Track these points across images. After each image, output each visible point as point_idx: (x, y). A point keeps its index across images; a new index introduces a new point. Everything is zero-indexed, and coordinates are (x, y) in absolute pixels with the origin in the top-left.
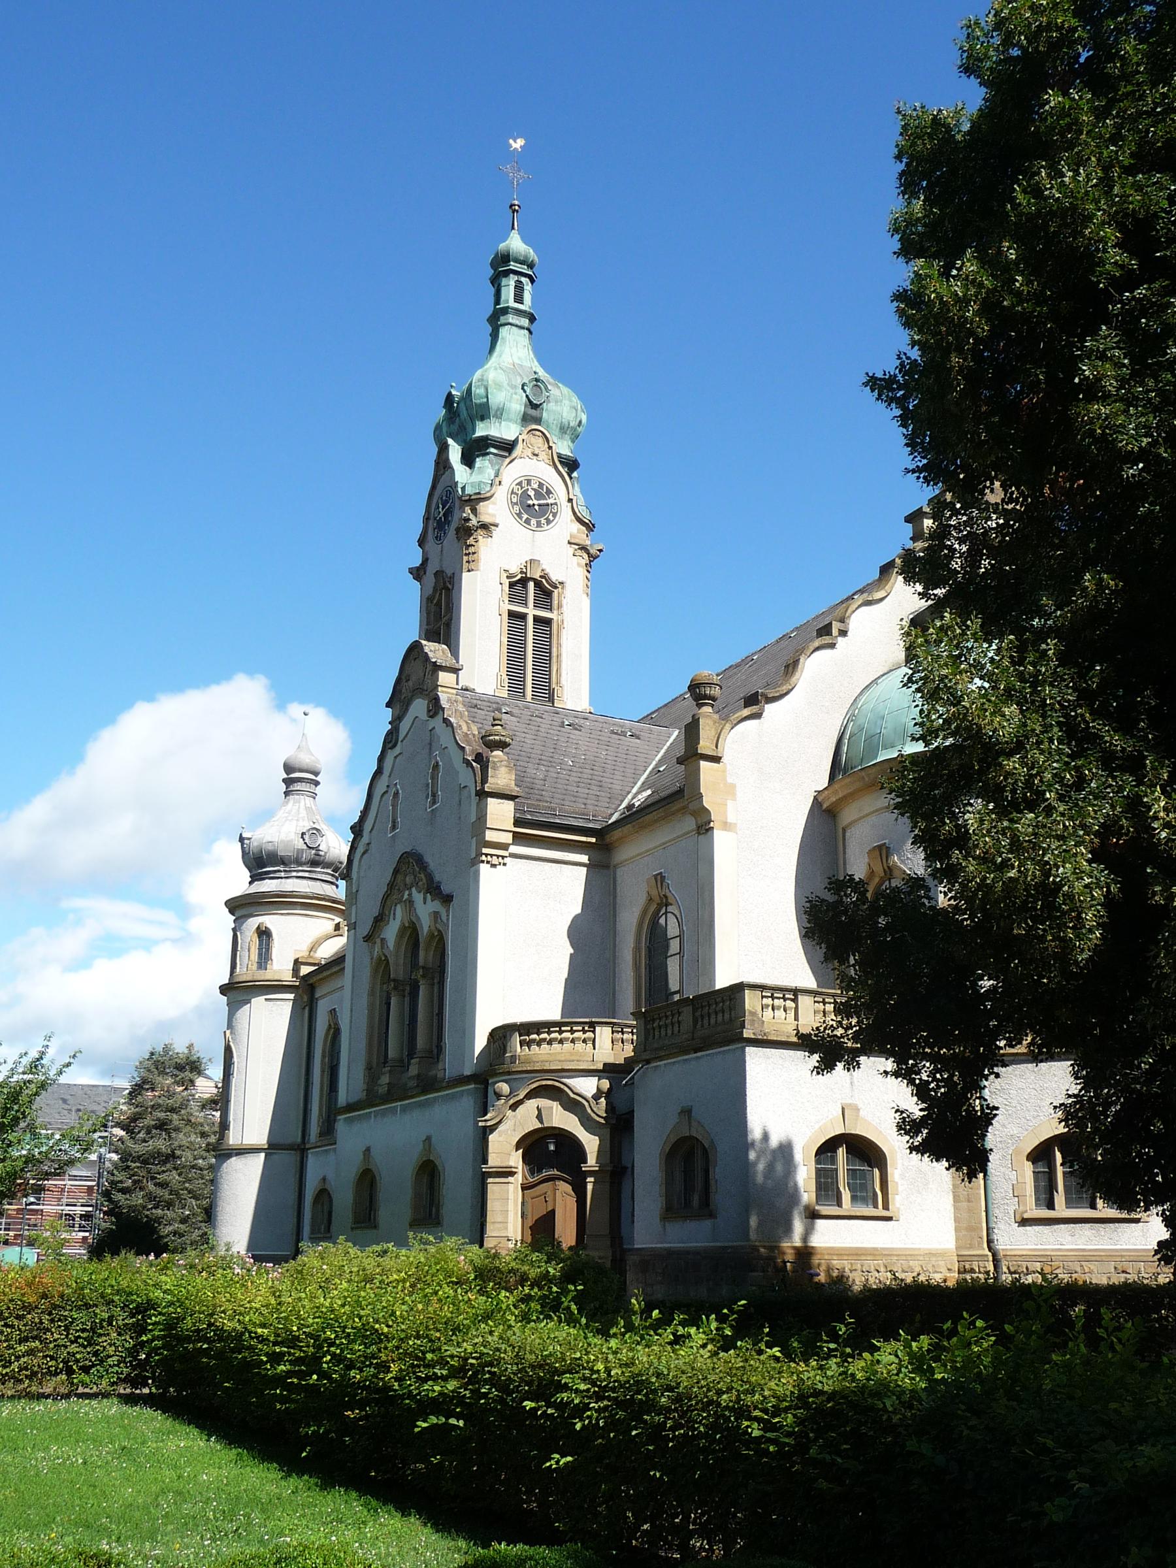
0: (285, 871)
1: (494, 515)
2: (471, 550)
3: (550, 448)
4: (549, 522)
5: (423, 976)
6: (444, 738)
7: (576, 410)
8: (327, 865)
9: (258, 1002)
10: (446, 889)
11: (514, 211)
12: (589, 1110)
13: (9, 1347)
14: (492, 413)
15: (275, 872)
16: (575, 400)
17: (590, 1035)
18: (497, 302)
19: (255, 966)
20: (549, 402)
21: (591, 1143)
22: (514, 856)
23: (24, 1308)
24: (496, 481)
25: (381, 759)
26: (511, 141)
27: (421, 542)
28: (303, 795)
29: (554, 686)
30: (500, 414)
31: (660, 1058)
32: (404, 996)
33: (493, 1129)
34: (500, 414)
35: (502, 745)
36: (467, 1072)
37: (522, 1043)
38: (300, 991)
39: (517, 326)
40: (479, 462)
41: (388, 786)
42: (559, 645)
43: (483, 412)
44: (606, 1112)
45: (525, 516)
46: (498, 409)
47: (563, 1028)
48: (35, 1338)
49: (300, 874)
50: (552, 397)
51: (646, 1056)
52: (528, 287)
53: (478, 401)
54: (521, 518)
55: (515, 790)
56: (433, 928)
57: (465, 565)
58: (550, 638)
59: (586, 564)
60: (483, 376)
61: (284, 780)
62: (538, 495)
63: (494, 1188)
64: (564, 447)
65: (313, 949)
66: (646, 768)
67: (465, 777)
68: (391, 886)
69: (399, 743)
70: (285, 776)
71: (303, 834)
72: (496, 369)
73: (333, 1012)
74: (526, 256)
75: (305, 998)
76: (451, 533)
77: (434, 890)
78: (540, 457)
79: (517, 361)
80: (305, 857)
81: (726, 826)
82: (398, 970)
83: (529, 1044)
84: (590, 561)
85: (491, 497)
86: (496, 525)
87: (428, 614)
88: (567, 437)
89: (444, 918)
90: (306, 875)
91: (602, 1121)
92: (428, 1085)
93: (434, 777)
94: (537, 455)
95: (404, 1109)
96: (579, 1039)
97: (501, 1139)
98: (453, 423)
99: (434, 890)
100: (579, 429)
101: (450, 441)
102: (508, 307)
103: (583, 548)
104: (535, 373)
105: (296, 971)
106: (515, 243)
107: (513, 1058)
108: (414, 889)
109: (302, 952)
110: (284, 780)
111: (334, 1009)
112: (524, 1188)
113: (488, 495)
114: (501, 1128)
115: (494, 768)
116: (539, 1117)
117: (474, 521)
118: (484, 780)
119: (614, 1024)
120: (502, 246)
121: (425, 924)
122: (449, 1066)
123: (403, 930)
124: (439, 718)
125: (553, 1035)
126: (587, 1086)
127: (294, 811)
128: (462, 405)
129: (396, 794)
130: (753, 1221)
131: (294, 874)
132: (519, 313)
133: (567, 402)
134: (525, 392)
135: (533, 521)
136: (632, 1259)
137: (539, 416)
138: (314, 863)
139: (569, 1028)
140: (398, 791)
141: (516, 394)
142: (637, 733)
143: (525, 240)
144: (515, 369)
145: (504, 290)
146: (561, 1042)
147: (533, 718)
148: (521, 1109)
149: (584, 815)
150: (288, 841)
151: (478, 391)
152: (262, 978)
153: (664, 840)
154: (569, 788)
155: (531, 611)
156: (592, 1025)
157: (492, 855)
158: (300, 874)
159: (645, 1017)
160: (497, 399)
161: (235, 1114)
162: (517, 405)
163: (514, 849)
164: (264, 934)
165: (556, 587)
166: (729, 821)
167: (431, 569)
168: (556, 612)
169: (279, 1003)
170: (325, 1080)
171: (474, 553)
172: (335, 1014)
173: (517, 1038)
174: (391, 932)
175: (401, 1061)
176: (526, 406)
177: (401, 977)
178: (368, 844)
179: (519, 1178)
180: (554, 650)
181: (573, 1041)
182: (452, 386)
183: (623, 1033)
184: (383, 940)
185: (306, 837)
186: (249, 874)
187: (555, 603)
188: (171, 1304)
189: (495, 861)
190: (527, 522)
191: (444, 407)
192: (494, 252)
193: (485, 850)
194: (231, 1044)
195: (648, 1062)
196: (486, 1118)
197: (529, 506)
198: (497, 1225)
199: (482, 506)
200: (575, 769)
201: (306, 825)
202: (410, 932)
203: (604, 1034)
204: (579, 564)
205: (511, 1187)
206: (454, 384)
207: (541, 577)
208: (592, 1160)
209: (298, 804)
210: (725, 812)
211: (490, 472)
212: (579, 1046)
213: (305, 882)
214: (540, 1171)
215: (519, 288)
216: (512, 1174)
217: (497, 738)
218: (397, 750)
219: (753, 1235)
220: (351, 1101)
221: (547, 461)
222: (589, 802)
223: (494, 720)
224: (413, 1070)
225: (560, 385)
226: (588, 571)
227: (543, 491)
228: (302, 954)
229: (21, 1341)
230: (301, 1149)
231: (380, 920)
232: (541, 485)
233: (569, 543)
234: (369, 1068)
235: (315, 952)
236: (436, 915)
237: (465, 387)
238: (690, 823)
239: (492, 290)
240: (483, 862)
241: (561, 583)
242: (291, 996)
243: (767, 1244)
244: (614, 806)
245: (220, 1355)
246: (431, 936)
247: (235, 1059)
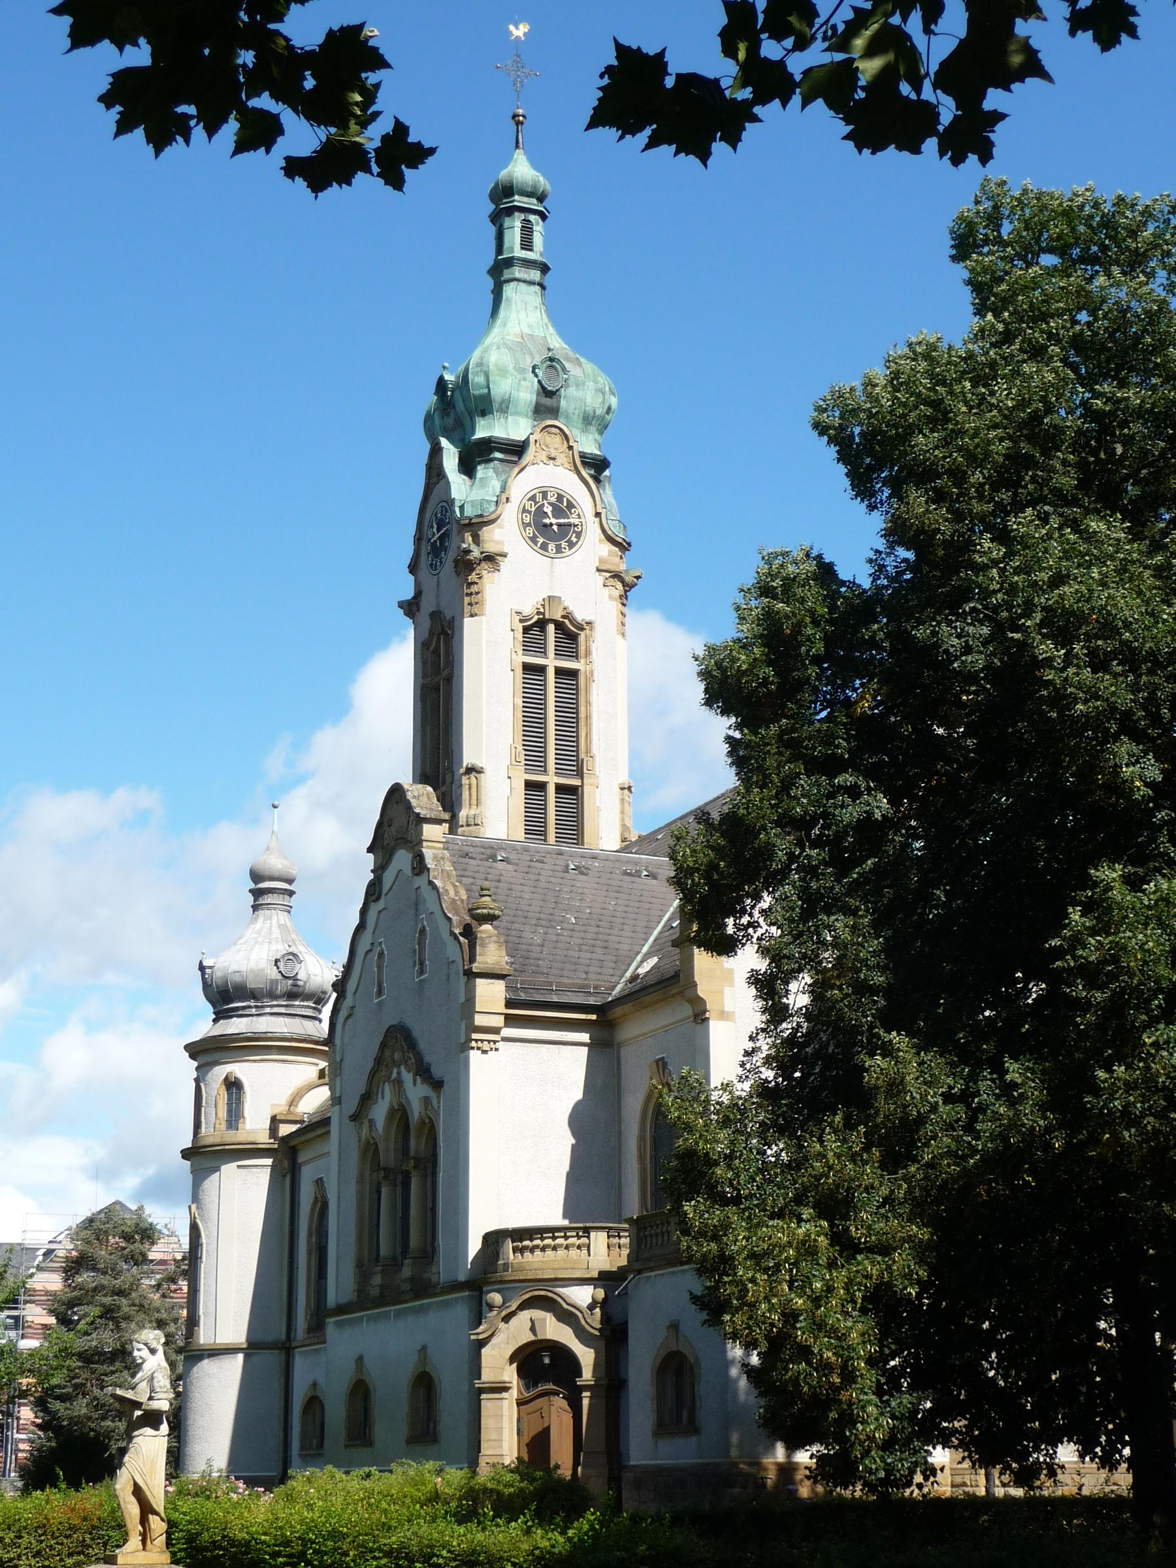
0: (256, 1007)
1: (501, 542)
2: (474, 589)
3: (570, 448)
4: (571, 545)
5: (416, 1167)
6: (430, 903)
7: (604, 394)
8: (308, 997)
9: (229, 1169)
10: (437, 1072)
11: (518, 123)
12: (583, 1322)
13: (61, 1560)
14: (495, 406)
15: (244, 1008)
16: (603, 380)
17: (584, 1240)
18: (500, 249)
19: (224, 1126)
20: (568, 386)
21: (586, 1356)
22: (505, 1039)
23: (70, 1529)
24: (502, 498)
25: (364, 912)
26: (512, 27)
27: (413, 568)
28: (275, 909)
29: (582, 755)
30: (505, 407)
31: (651, 1269)
32: (396, 1186)
33: (482, 1343)
34: (505, 407)
35: (490, 918)
36: (462, 1278)
37: (515, 1250)
38: (280, 1156)
39: (525, 281)
40: (481, 471)
41: (372, 944)
42: (588, 703)
43: (485, 406)
44: (602, 1323)
45: (541, 540)
46: (503, 401)
47: (556, 1234)
48: (79, 1553)
49: (275, 1010)
50: (572, 379)
51: (637, 1266)
52: (538, 227)
53: (477, 392)
54: (535, 543)
55: (506, 969)
56: (423, 1114)
57: (467, 609)
58: (577, 694)
59: (621, 596)
60: (482, 358)
61: (251, 891)
62: (558, 511)
63: (488, 1405)
64: (588, 444)
65: (293, 1102)
66: (661, 917)
67: (452, 951)
68: (378, 1061)
69: (383, 896)
70: (252, 886)
71: (277, 961)
72: (498, 348)
73: (319, 1182)
74: (535, 187)
75: (286, 1163)
76: (449, 565)
77: (424, 1072)
78: (558, 462)
79: (526, 330)
80: (281, 988)
81: (724, 1015)
82: (388, 1157)
83: (522, 1250)
84: (626, 591)
85: (498, 518)
86: (504, 555)
87: (424, 663)
88: (593, 429)
89: (435, 1105)
90: (283, 1010)
91: (597, 1333)
92: (423, 1288)
93: (421, 943)
94: (554, 459)
95: (398, 1314)
96: (573, 1245)
97: (494, 1353)
98: (448, 415)
99: (424, 1072)
100: (608, 417)
101: (444, 442)
102: (513, 258)
103: (617, 576)
104: (549, 349)
105: (273, 1130)
106: (521, 169)
107: (506, 1266)
108: (403, 1068)
109: (279, 1103)
110: (251, 891)
111: (321, 1179)
112: (520, 1403)
113: (493, 517)
114: (494, 1341)
115: (482, 946)
116: (533, 1329)
117: (476, 553)
118: (472, 959)
119: (610, 1228)
120: (503, 174)
121: (416, 1111)
122: (443, 1271)
123: (392, 1113)
124: (424, 877)
125: (547, 1242)
126: (582, 1296)
127: (265, 930)
128: (457, 395)
129: (381, 955)
130: (735, 1438)
131: (268, 1010)
132: (528, 264)
133: (591, 384)
134: (536, 376)
135: (552, 546)
136: (627, 1476)
137: (555, 405)
138: (292, 995)
139: (563, 1234)
140: (383, 950)
141: (525, 379)
142: (655, 871)
143: (535, 164)
144: (522, 345)
145: (507, 235)
146: (555, 1248)
147: (534, 864)
148: (514, 1321)
149: (582, 989)
150: (259, 970)
151: (477, 379)
152: (234, 1140)
153: (665, 1023)
154: (571, 953)
155: (551, 662)
156: (587, 1231)
157: (482, 1041)
158: (275, 1010)
159: (637, 1224)
160: (501, 388)
161: (206, 1306)
162: (527, 394)
163: (507, 1032)
164: (233, 1086)
165: (582, 629)
166: (726, 1009)
167: (427, 605)
168: (583, 661)
169: (254, 1170)
170: (313, 1263)
171: (477, 593)
172: (323, 1185)
173: (509, 1245)
174: (380, 1112)
175: (394, 1258)
176: (538, 394)
177: (391, 1163)
178: (352, 1008)
179: (514, 1393)
180: (582, 709)
181: (567, 1247)
182: (444, 367)
183: (620, 1237)
184: (371, 1122)
185: (281, 964)
186: (212, 1010)
187: (582, 648)
188: (190, 1522)
189: (486, 1046)
190: (544, 547)
191: (436, 393)
192: (495, 181)
193: (474, 1036)
194: (198, 1221)
195: (640, 1272)
196: (478, 1330)
197: (545, 525)
198: (490, 1443)
199: (485, 533)
200: (577, 928)
201: (280, 949)
202: (400, 1114)
203: (599, 1240)
204: (611, 597)
205: (505, 1403)
206: (447, 365)
207: (563, 617)
208: (587, 1374)
209: (273, 920)
210: (722, 1000)
211: (495, 484)
212: (574, 1252)
213: (281, 1019)
214: (535, 1385)
215: (527, 230)
216: (506, 1389)
217: (485, 911)
218: (381, 905)
219: (734, 1452)
220: (341, 1301)
221: (567, 466)
222: (592, 969)
223: (482, 889)
224: (407, 1272)
225: (582, 360)
226: (624, 605)
227: (563, 506)
228: (281, 1108)
229: (70, 1555)
230: (287, 1348)
231: (367, 1099)
232: (560, 498)
233: (598, 570)
234: (360, 1265)
235: (296, 1106)
236: (426, 1100)
237: (462, 368)
238: (687, 1010)
239: (492, 230)
240: (473, 1048)
241: (588, 623)
242: (269, 1161)
243: (746, 1460)
244: (619, 973)
245: (234, 1558)
246: (422, 1123)
247: (204, 1240)
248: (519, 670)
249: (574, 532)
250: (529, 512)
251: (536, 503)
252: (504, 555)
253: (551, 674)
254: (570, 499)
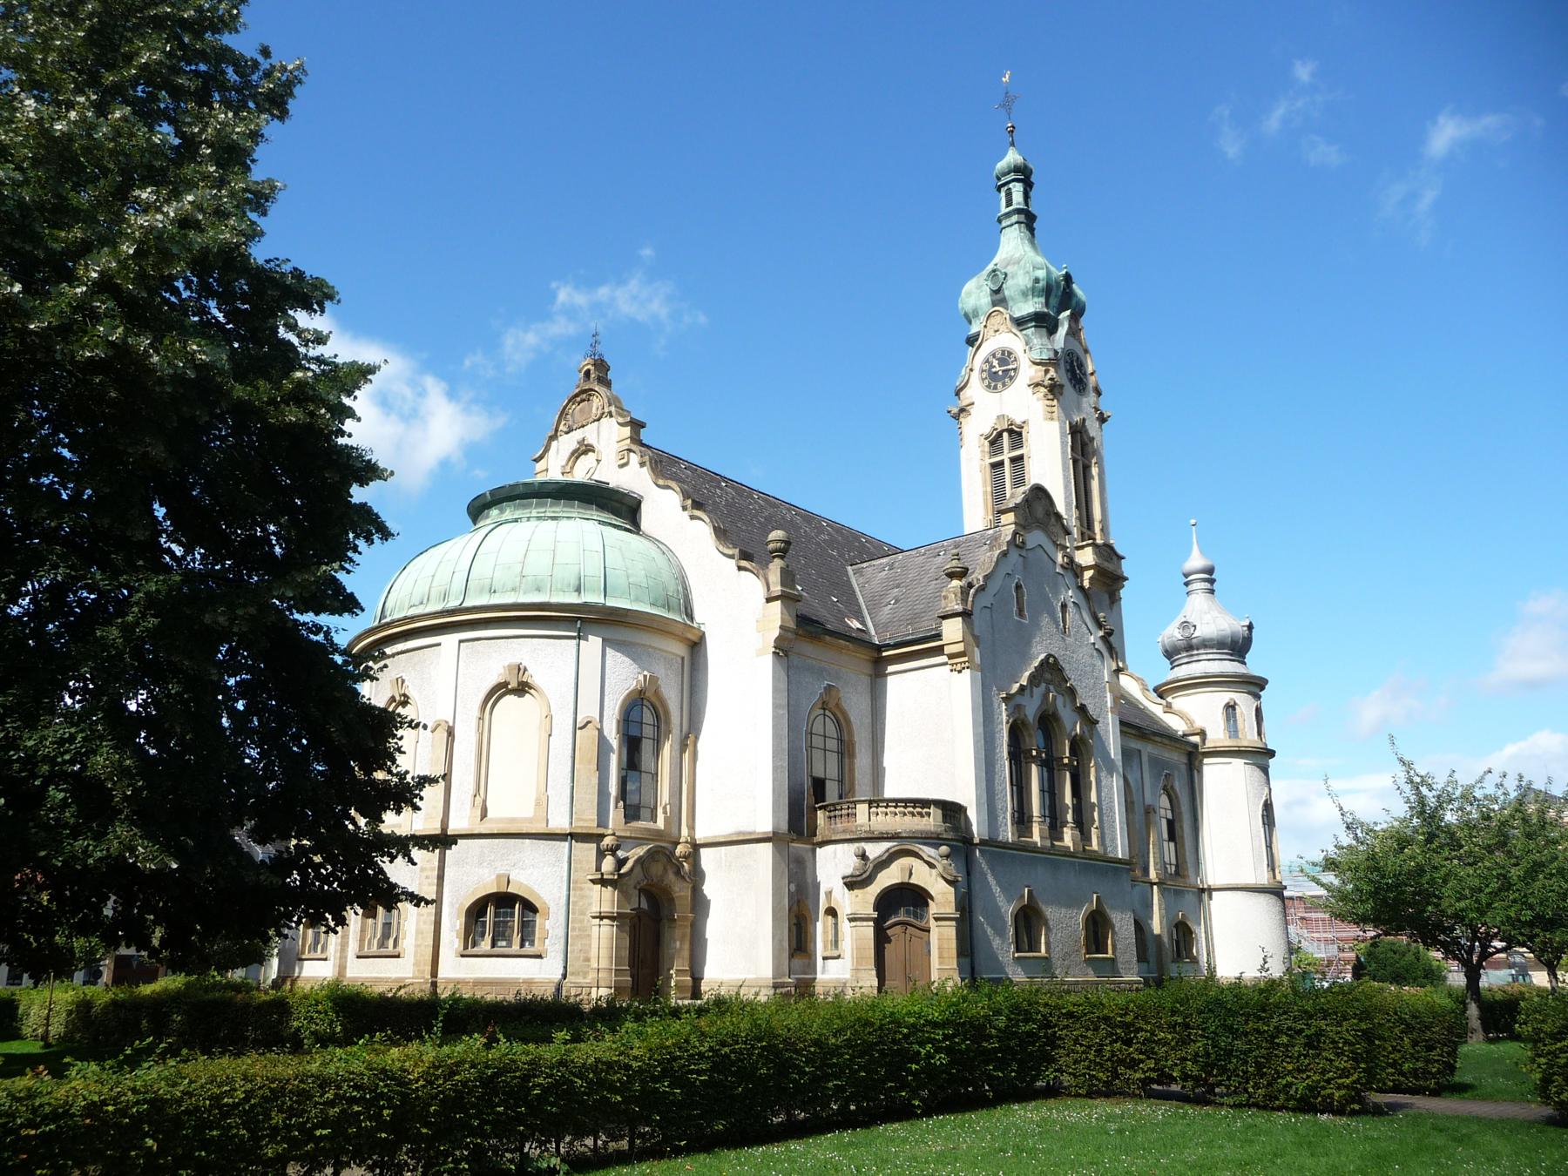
1: (971, 397)
62: (1003, 362)
135: (1000, 385)
165: (1022, 428)
248: (988, 468)
253: (1007, 463)
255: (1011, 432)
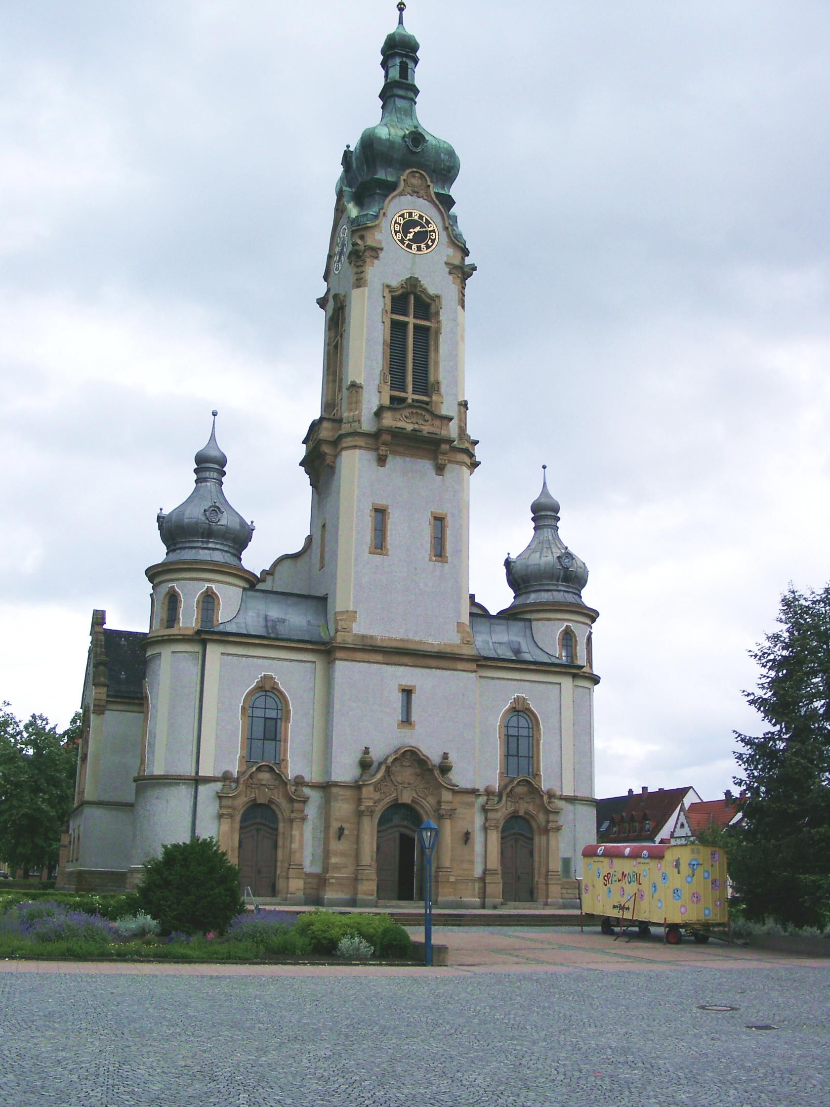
1: (380, 242)
4: (428, 247)
86: (382, 249)
155: (411, 320)
232: (421, 217)
249: (430, 238)
250: (400, 224)
251: (404, 219)
252: (382, 249)
254: (427, 217)
255: (418, 299)
